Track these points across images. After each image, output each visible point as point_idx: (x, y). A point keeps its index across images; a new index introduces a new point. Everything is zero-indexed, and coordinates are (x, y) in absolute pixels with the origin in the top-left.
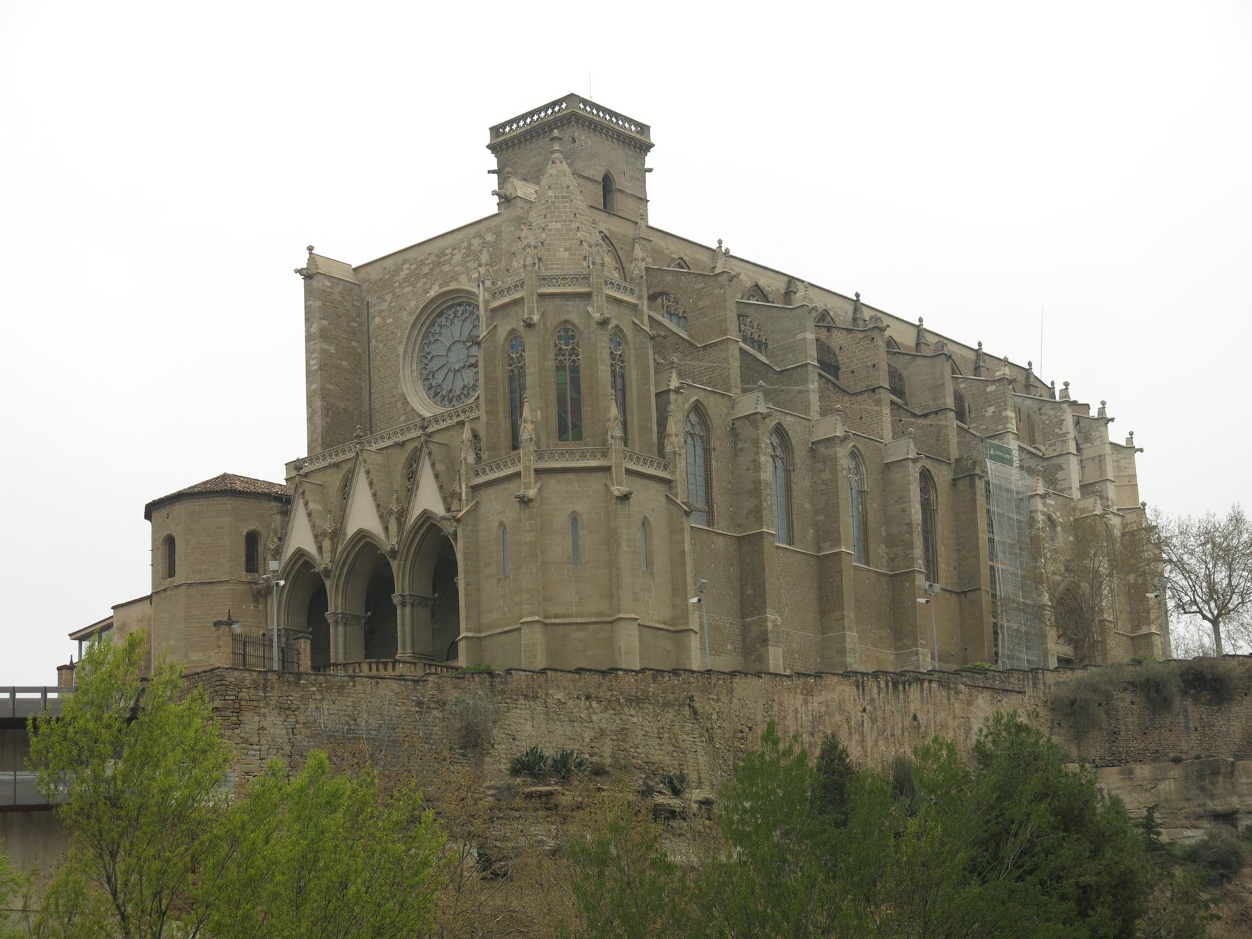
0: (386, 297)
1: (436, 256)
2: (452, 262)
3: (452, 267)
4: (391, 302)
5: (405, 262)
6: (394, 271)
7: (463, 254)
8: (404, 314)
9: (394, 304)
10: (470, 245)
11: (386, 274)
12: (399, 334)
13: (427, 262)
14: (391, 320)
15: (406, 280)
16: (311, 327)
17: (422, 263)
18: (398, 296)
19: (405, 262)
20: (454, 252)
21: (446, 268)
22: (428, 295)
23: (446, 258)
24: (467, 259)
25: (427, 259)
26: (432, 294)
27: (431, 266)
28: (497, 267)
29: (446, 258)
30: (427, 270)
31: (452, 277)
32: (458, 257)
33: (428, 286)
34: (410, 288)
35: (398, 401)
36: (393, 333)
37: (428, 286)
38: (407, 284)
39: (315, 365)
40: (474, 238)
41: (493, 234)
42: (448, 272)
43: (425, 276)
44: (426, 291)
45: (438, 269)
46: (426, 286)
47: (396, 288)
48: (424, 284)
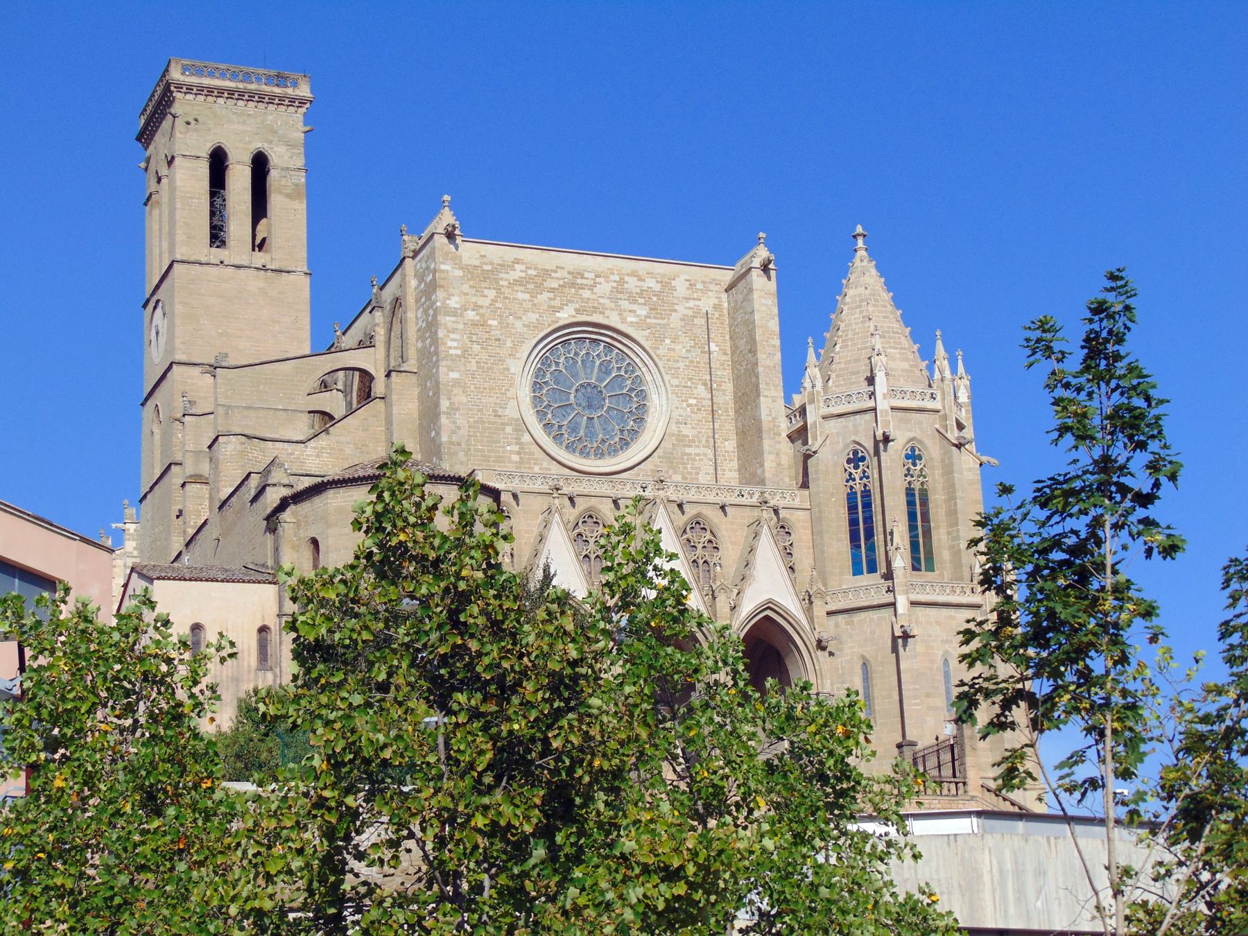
0: (486, 292)
1: (569, 273)
2: (595, 290)
3: (595, 297)
4: (494, 301)
5: (517, 261)
6: (498, 265)
7: (613, 287)
8: (518, 324)
9: (497, 305)
10: (622, 282)
11: (486, 264)
12: (509, 344)
13: (553, 275)
14: (495, 323)
15: (519, 282)
16: (449, 299)
17: (546, 273)
18: (506, 298)
19: (517, 261)
20: (598, 280)
21: (586, 294)
22: (558, 315)
23: (584, 282)
24: (619, 296)
25: (556, 272)
26: (565, 316)
27: (561, 282)
28: (664, 322)
29: (584, 282)
30: (555, 285)
31: (594, 307)
32: (604, 287)
33: (557, 303)
34: (527, 296)
35: (507, 424)
36: (499, 340)
37: (557, 303)
38: (523, 289)
39: (455, 348)
40: (628, 275)
41: (657, 282)
42: (588, 299)
43: (552, 290)
44: (556, 310)
45: (573, 291)
46: (553, 303)
47: (503, 286)
48: (550, 299)
